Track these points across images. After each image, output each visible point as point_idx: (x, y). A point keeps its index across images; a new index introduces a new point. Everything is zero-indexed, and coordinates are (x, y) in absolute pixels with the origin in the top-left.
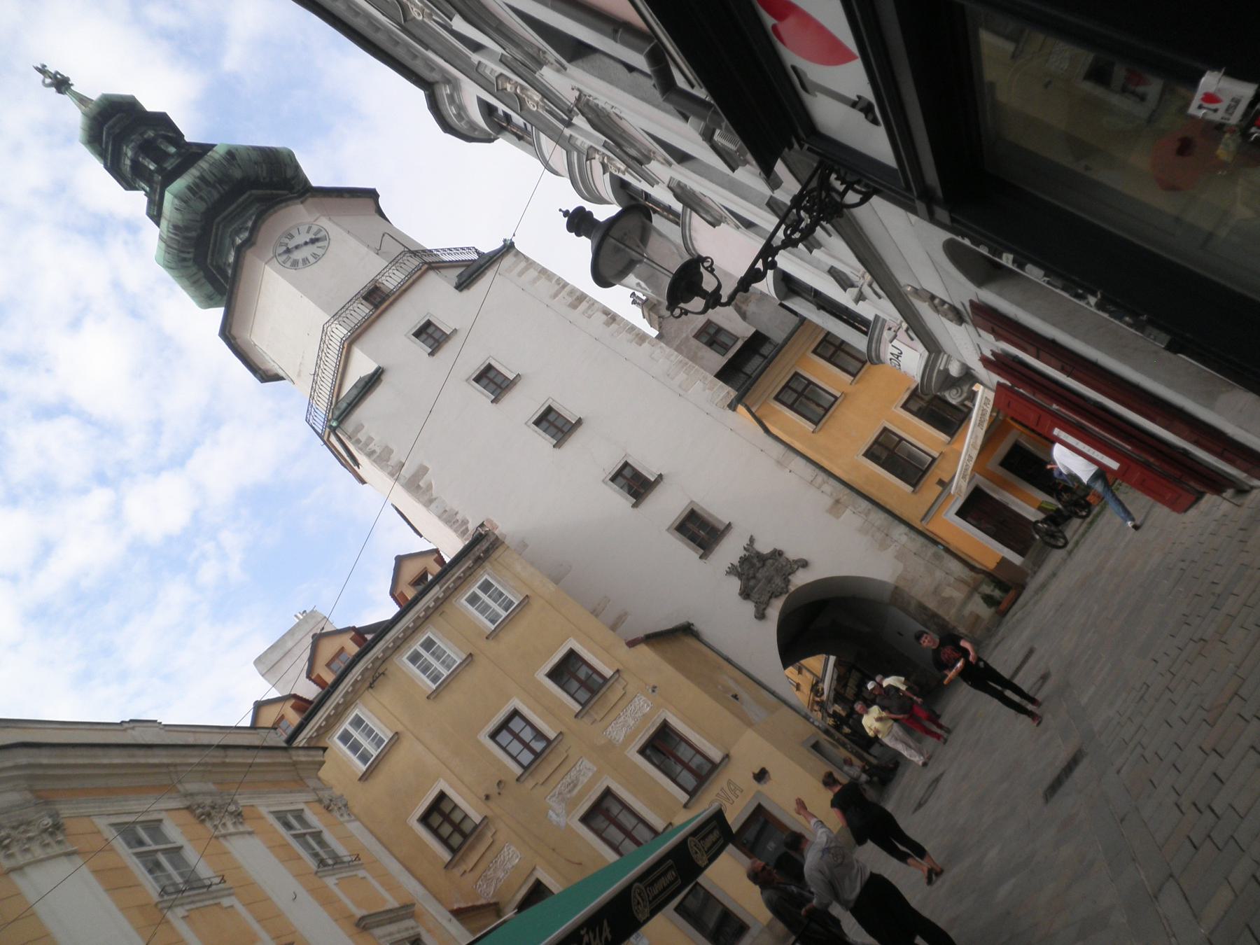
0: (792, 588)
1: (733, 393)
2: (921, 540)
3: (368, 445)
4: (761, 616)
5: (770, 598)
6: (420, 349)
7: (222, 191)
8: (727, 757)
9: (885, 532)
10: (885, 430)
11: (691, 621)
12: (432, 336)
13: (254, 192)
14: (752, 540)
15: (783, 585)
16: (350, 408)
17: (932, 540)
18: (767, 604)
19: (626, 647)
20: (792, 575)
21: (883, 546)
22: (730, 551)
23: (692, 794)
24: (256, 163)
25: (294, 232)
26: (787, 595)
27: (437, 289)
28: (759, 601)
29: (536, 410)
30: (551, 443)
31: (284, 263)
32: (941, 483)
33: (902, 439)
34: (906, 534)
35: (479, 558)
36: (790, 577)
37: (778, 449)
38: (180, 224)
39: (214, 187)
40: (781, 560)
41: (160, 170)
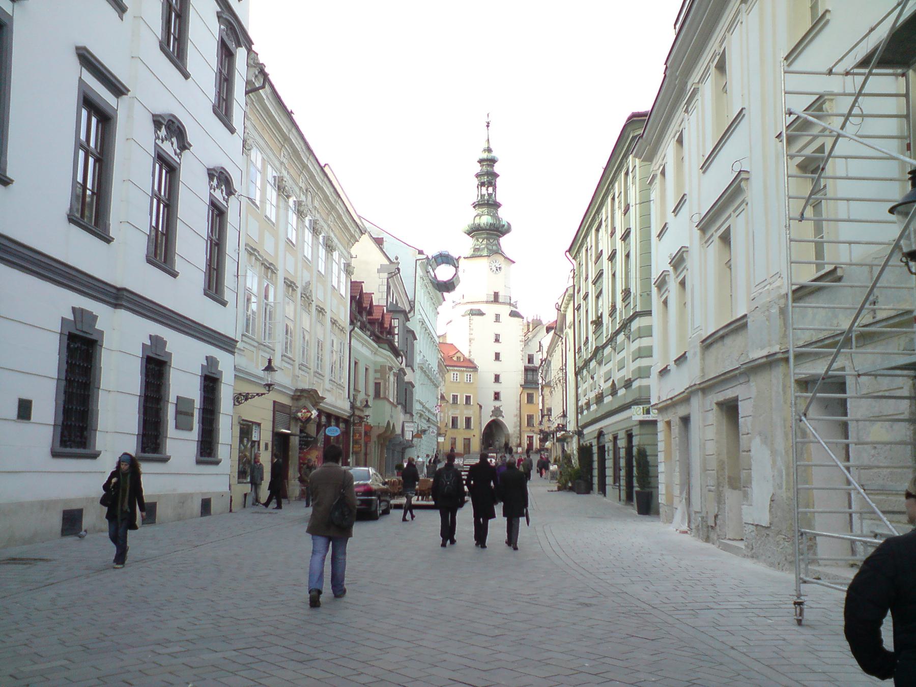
4: (491, 416)
6: (494, 319)
12: (497, 318)
21: (514, 427)
22: (497, 404)
23: (466, 428)
27: (506, 310)
41: (488, 201)
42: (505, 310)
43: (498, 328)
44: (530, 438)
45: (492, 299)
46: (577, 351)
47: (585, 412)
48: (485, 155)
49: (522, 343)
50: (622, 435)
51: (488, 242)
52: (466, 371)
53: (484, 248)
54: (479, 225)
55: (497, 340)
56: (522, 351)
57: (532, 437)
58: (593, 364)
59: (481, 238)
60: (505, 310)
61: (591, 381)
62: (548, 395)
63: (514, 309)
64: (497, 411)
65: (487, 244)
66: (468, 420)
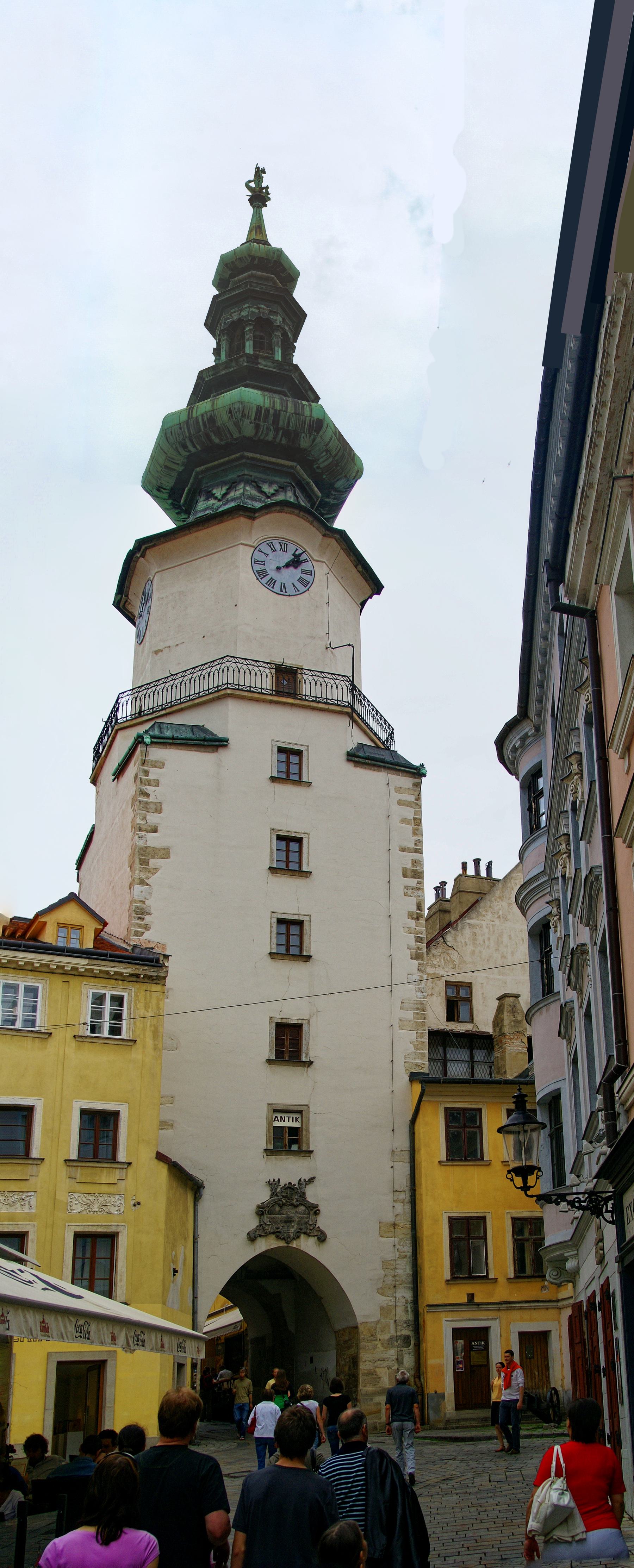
0: (294, 1244)
2: (410, 1316)
3: (149, 785)
5: (273, 1233)
7: (278, 440)
9: (397, 1283)
10: (484, 1219)
11: (205, 1184)
13: (299, 467)
14: (311, 1180)
15: (292, 1235)
16: (171, 741)
17: (417, 1325)
18: (266, 1235)
19: (154, 1155)
20: (306, 1236)
24: (327, 451)
26: (286, 1245)
28: (264, 1226)
29: (291, 911)
30: (271, 948)
31: (257, 562)
33: (485, 1238)
34: (407, 1301)
35: (137, 976)
36: (302, 1236)
37: (403, 1142)
38: (219, 423)
39: (277, 430)
40: (312, 1217)
41: (253, 359)
52: (89, 974)
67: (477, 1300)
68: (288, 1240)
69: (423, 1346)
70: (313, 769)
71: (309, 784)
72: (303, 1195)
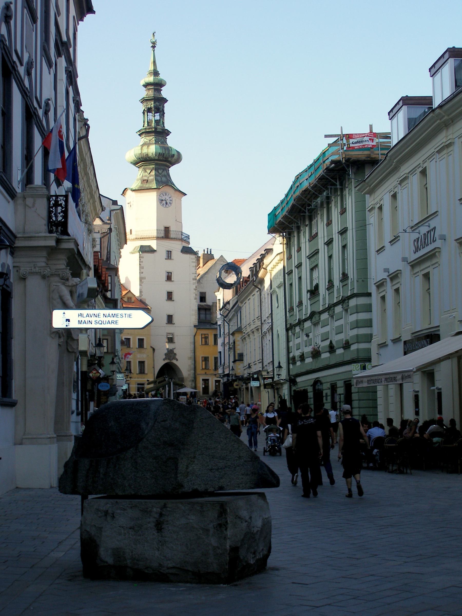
0: (172, 361)
1: (197, 324)
2: (194, 376)
4: (164, 360)
6: (165, 255)
8: (147, 374)
12: (169, 254)
14: (175, 348)
17: (195, 378)
23: (139, 373)
25: (167, 194)
32: (206, 373)
39: (163, 158)
41: (156, 128)
42: (176, 247)
43: (169, 266)
44: (206, 381)
45: (162, 235)
46: (288, 310)
47: (298, 363)
48: (151, 79)
49: (195, 281)
50: (340, 384)
51: (157, 173)
53: (152, 180)
54: (147, 155)
55: (169, 278)
56: (196, 290)
57: (208, 380)
58: (308, 324)
59: (149, 169)
60: (176, 247)
61: (305, 338)
62: (238, 341)
63: (186, 245)
64: (170, 354)
65: (156, 175)
66: (142, 364)
67: (207, 373)
68: (171, 360)
69: (196, 382)
70: (174, 255)
71: (173, 259)
72: (173, 351)
